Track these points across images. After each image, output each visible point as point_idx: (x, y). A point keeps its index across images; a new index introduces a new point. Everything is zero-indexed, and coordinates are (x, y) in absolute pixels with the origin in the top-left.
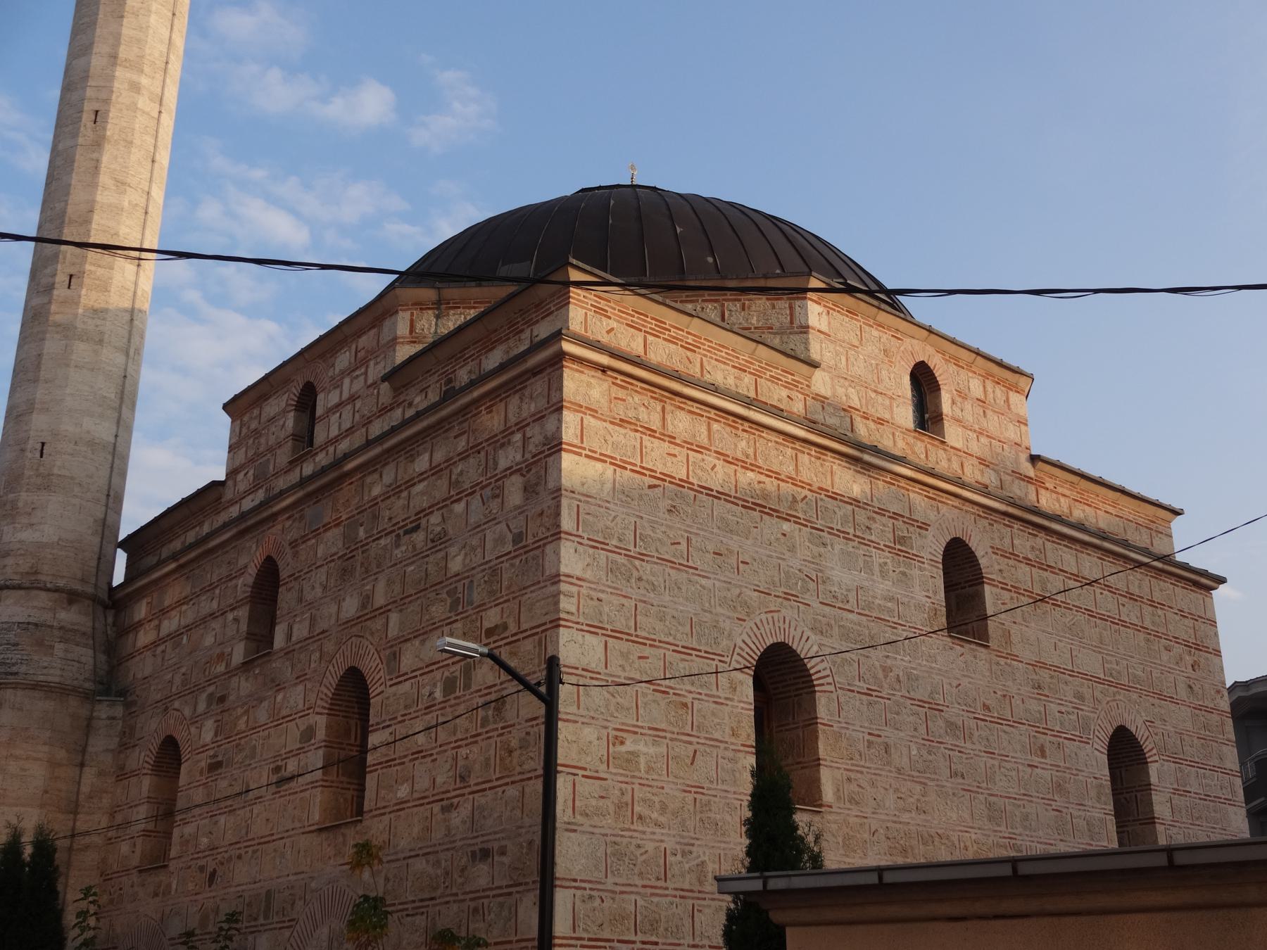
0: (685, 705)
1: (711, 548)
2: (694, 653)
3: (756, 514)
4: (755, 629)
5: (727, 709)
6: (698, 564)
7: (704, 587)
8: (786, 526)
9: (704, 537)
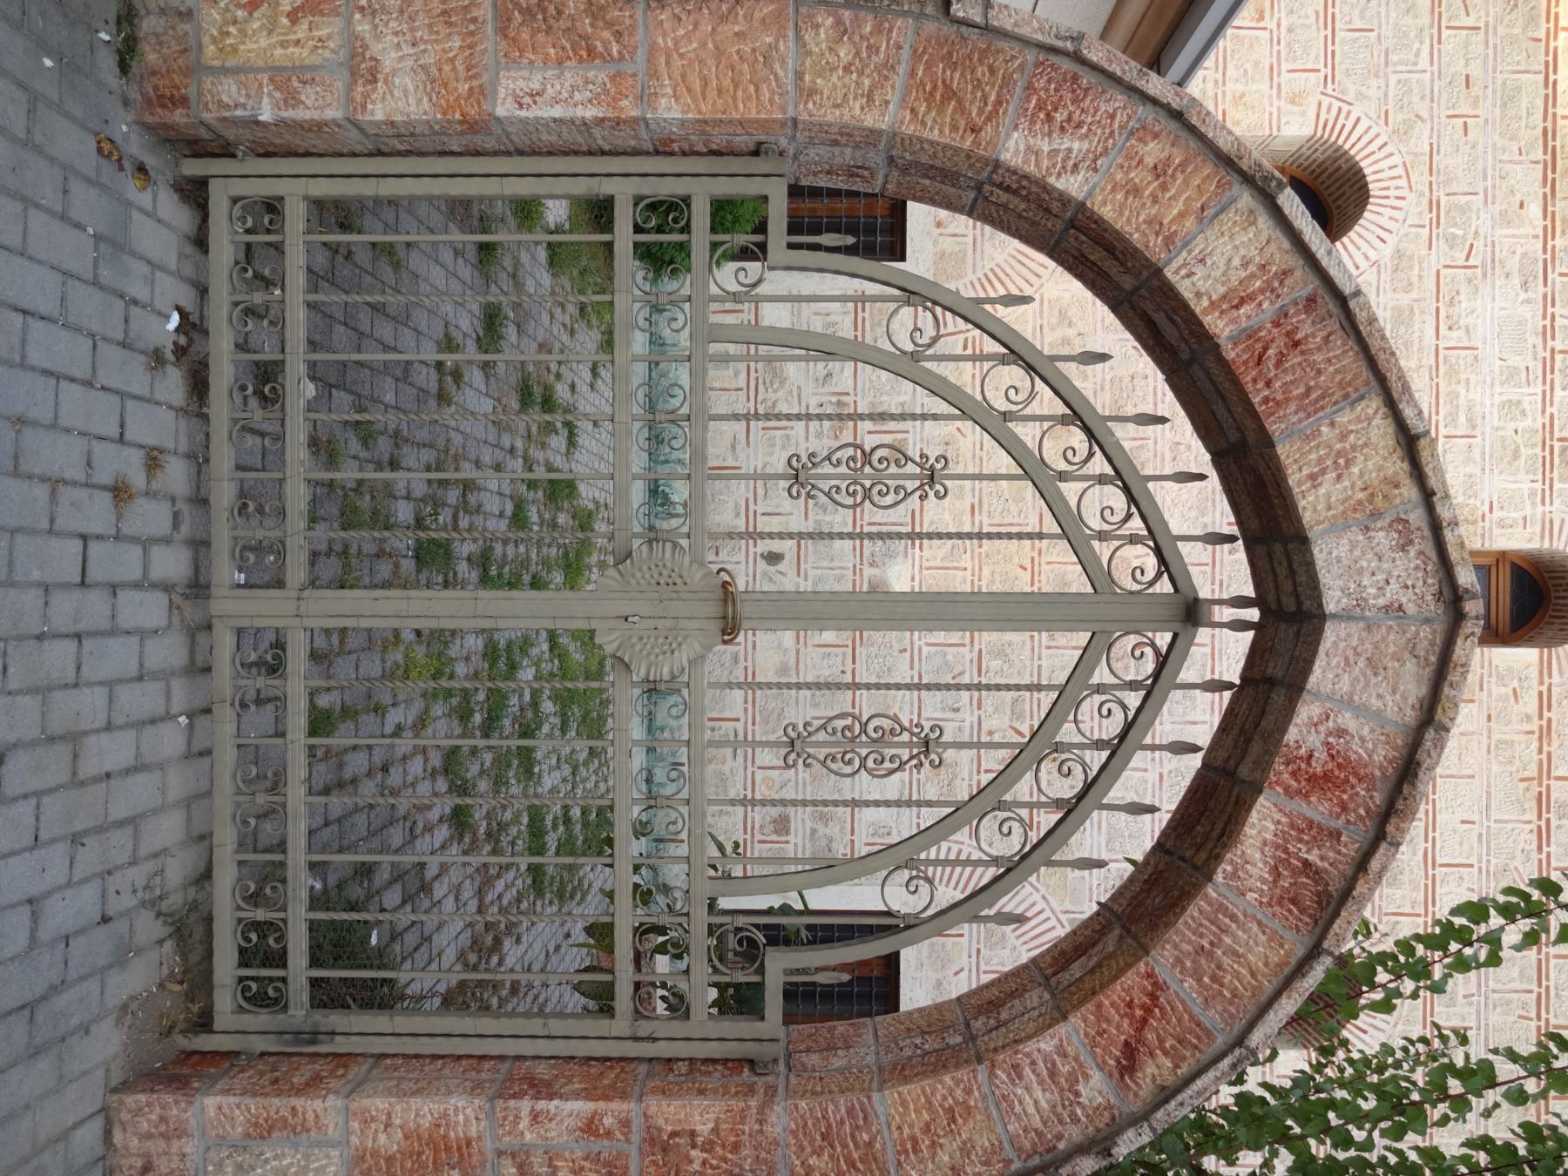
0: (1261, 18)
1: (1475, 70)
2: (1329, 32)
3: (1539, 155)
4: (1378, 142)
5: (1265, 87)
6: (1447, 47)
7: (1417, 55)
8: (1535, 209)
9: (1486, 56)
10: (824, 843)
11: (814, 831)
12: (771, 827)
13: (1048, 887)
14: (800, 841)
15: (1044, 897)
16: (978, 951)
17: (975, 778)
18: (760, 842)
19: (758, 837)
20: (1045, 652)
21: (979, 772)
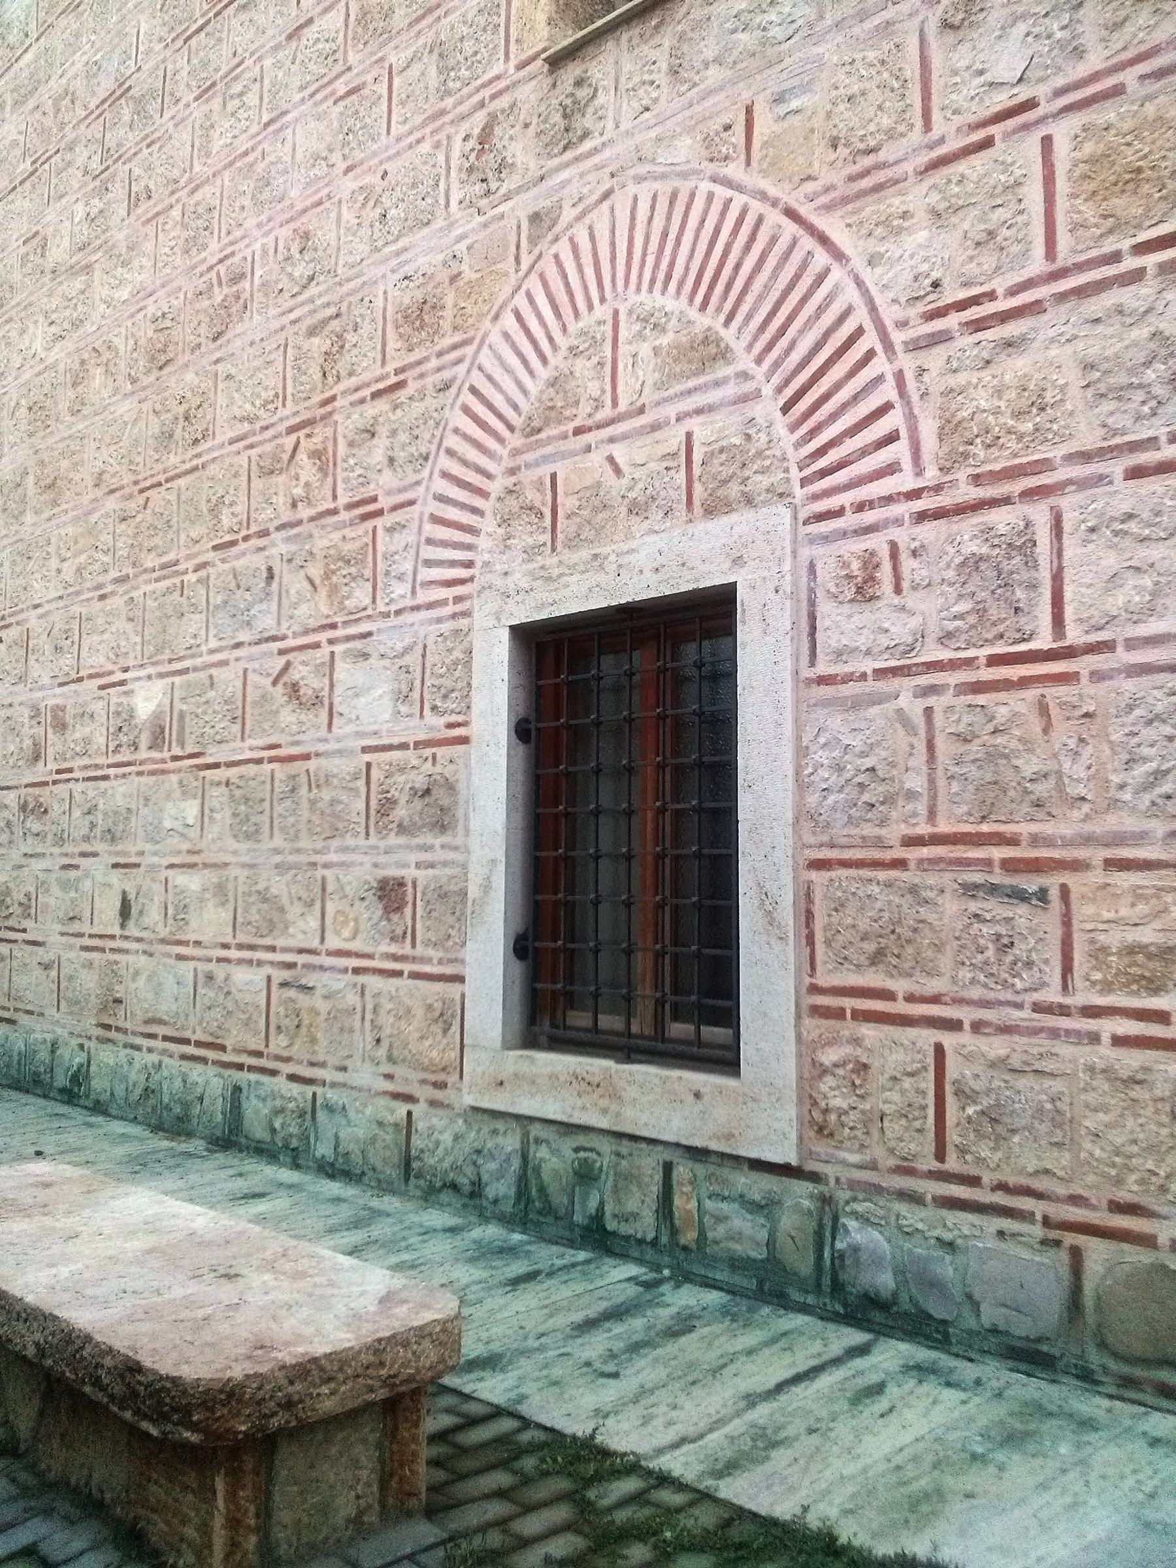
10: (418, 804)
11: (402, 829)
12: (395, 917)
13: (481, 316)
14: (413, 857)
15: (496, 317)
16: (578, 431)
17: (344, 516)
18: (414, 945)
19: (407, 949)
20: (219, 439)
21: (334, 512)
